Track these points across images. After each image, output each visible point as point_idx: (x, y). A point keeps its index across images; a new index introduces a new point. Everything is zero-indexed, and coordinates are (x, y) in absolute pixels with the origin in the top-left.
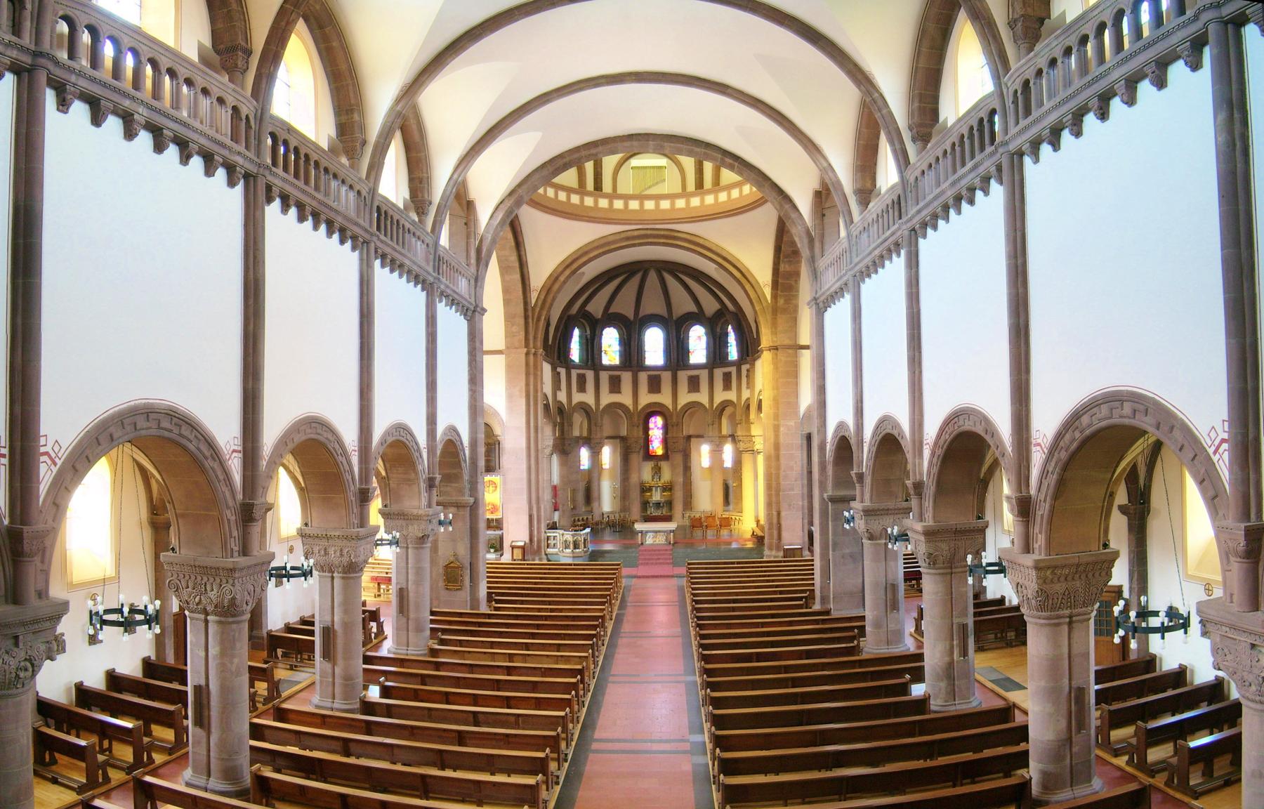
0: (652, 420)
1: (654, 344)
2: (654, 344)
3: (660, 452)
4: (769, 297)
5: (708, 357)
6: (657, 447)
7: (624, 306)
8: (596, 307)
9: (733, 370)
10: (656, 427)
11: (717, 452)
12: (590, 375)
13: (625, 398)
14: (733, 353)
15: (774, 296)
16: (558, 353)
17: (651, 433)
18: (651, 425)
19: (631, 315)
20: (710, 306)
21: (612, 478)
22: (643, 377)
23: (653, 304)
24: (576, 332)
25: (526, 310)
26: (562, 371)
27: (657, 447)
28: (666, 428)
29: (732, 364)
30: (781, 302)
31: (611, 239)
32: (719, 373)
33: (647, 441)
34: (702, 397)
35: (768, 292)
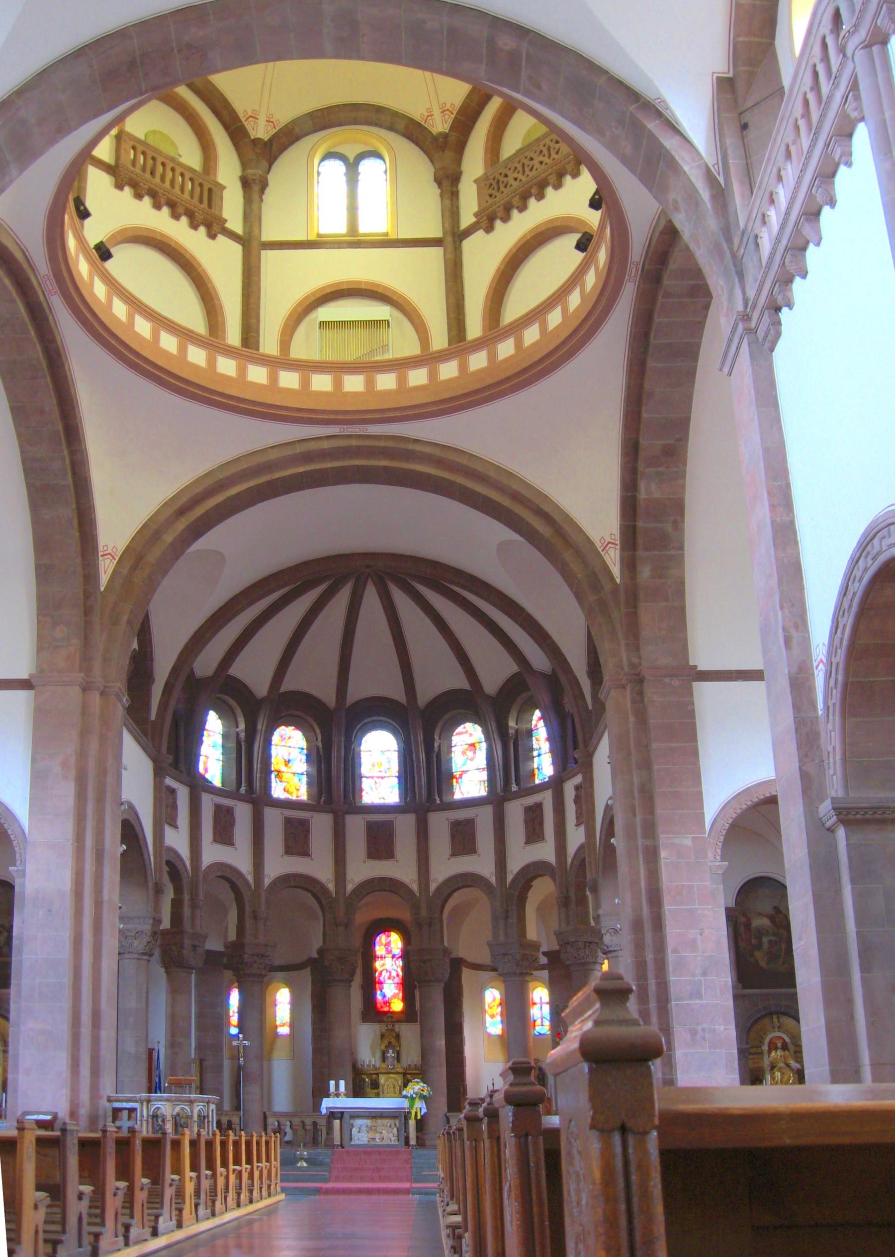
0: (383, 938)
1: (379, 760)
2: (379, 760)
3: (397, 1006)
4: (616, 571)
5: (491, 780)
6: (390, 993)
7: (314, 675)
8: (256, 669)
9: (547, 798)
10: (389, 955)
11: (516, 1009)
12: (243, 812)
13: (319, 866)
14: (544, 766)
15: (630, 565)
16: (174, 752)
17: (378, 964)
18: (380, 950)
19: (328, 696)
20: (494, 669)
21: (294, 1056)
22: (355, 826)
23: (375, 676)
24: (214, 724)
25: (87, 595)
26: (183, 794)
27: (390, 993)
28: (405, 955)
29: (543, 787)
30: (645, 573)
31: (274, 455)
32: (515, 811)
33: (371, 983)
34: (482, 864)
35: (613, 559)
